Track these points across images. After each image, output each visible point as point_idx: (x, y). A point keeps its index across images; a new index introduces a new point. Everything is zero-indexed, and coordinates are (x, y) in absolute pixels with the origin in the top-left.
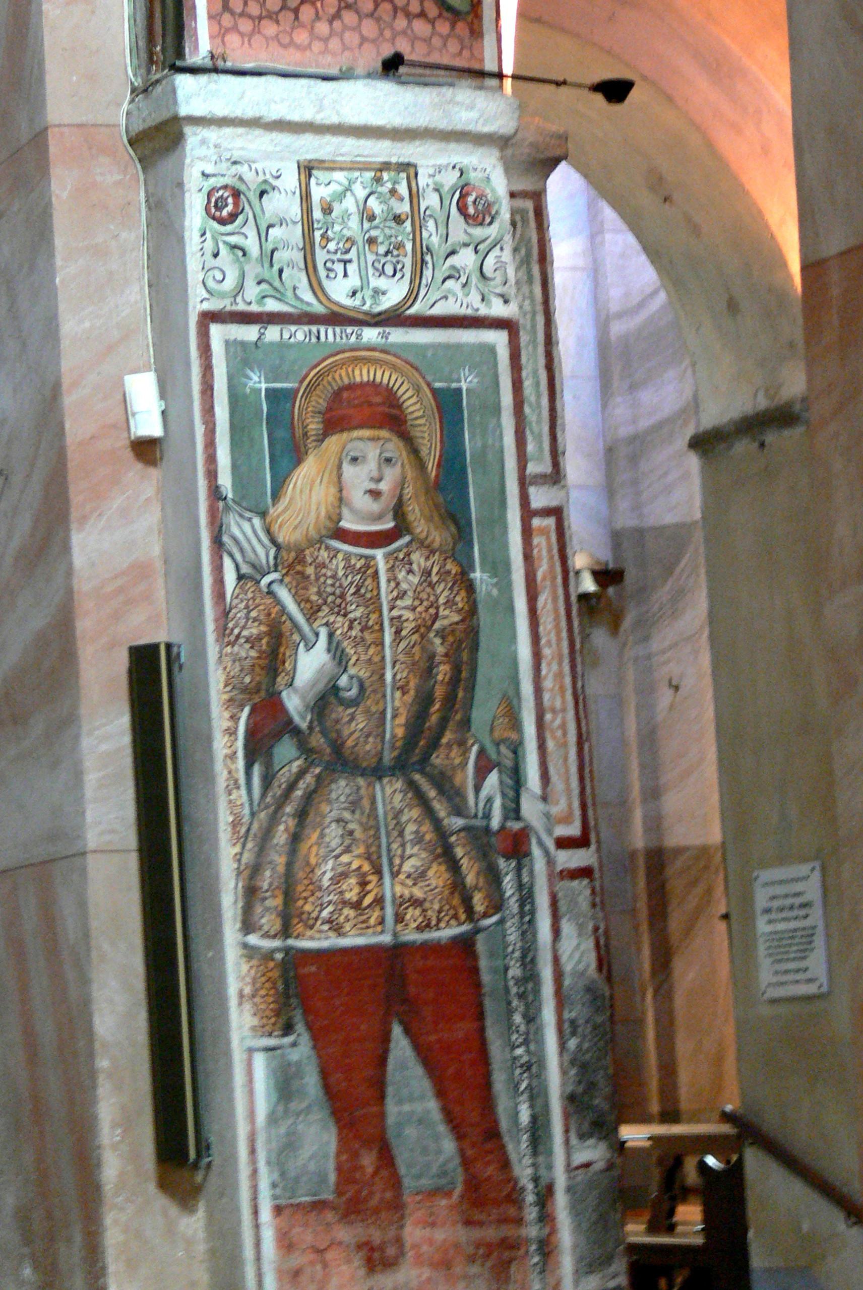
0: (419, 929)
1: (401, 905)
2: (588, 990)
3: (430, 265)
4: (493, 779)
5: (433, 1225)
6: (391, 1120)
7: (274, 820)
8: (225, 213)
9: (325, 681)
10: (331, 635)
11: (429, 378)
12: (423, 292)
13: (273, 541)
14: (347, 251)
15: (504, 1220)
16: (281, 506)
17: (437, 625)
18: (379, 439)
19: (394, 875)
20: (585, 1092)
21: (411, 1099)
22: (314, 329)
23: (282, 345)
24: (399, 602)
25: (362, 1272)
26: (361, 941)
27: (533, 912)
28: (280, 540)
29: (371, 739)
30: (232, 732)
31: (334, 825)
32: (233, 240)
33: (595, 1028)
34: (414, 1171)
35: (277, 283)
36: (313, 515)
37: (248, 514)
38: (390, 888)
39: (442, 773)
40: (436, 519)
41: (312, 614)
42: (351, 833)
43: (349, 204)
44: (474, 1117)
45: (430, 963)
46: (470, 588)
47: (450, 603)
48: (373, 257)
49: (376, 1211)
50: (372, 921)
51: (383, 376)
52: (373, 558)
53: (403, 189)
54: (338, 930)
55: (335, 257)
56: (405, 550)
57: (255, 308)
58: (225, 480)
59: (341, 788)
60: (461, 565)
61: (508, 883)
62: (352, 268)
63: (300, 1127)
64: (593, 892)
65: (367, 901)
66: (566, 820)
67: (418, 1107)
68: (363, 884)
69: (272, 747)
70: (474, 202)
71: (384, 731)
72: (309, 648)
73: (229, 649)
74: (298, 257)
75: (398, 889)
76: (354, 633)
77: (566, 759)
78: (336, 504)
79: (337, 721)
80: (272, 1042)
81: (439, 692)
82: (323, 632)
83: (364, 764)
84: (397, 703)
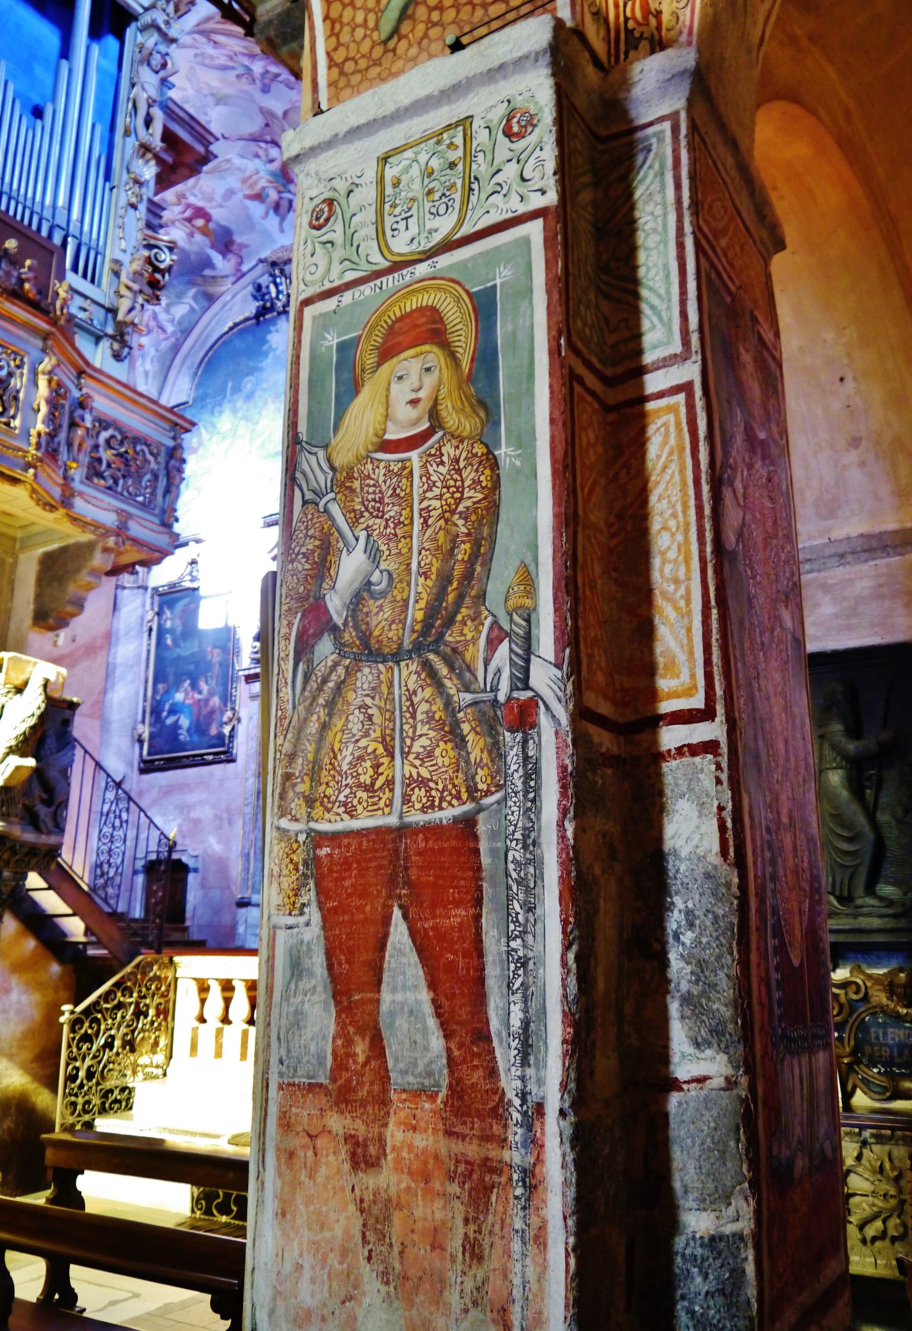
0: (424, 810)
1: (408, 785)
2: (708, 876)
3: (476, 192)
4: (504, 647)
5: (414, 1129)
6: (384, 1008)
7: (309, 711)
8: (322, 221)
9: (360, 579)
10: (369, 536)
11: (467, 287)
12: (469, 213)
13: (333, 468)
14: (410, 209)
15: (486, 1138)
16: (339, 436)
17: (461, 508)
18: (422, 354)
19: (405, 755)
20: (703, 993)
21: (404, 988)
22: (378, 282)
23: (355, 304)
24: (429, 495)
25: (347, 1166)
27: (537, 789)
28: (337, 465)
29: (394, 627)
31: (357, 712)
32: (324, 239)
33: (716, 917)
34: (402, 1066)
35: (355, 258)
36: (363, 436)
37: (315, 450)
38: (400, 769)
39: (454, 650)
40: (468, 409)
41: (354, 523)
42: (370, 718)
43: (415, 171)
44: (464, 1013)
45: (431, 844)
46: (494, 464)
48: (431, 204)
49: (363, 1104)
50: (382, 804)
51: (426, 300)
52: (409, 460)
54: (351, 813)
55: (398, 219)
56: (437, 446)
57: (337, 283)
59: (366, 676)
60: (487, 447)
61: (513, 757)
63: (306, 1006)
64: (719, 767)
65: (378, 784)
66: (689, 692)
67: (410, 996)
68: (376, 766)
69: (313, 646)
70: (518, 122)
71: (406, 618)
73: (290, 566)
75: (408, 769)
76: (388, 530)
77: (689, 630)
78: (382, 419)
79: (367, 614)
80: (291, 921)
81: (458, 570)
82: (363, 535)
83: (387, 651)
84: (420, 589)
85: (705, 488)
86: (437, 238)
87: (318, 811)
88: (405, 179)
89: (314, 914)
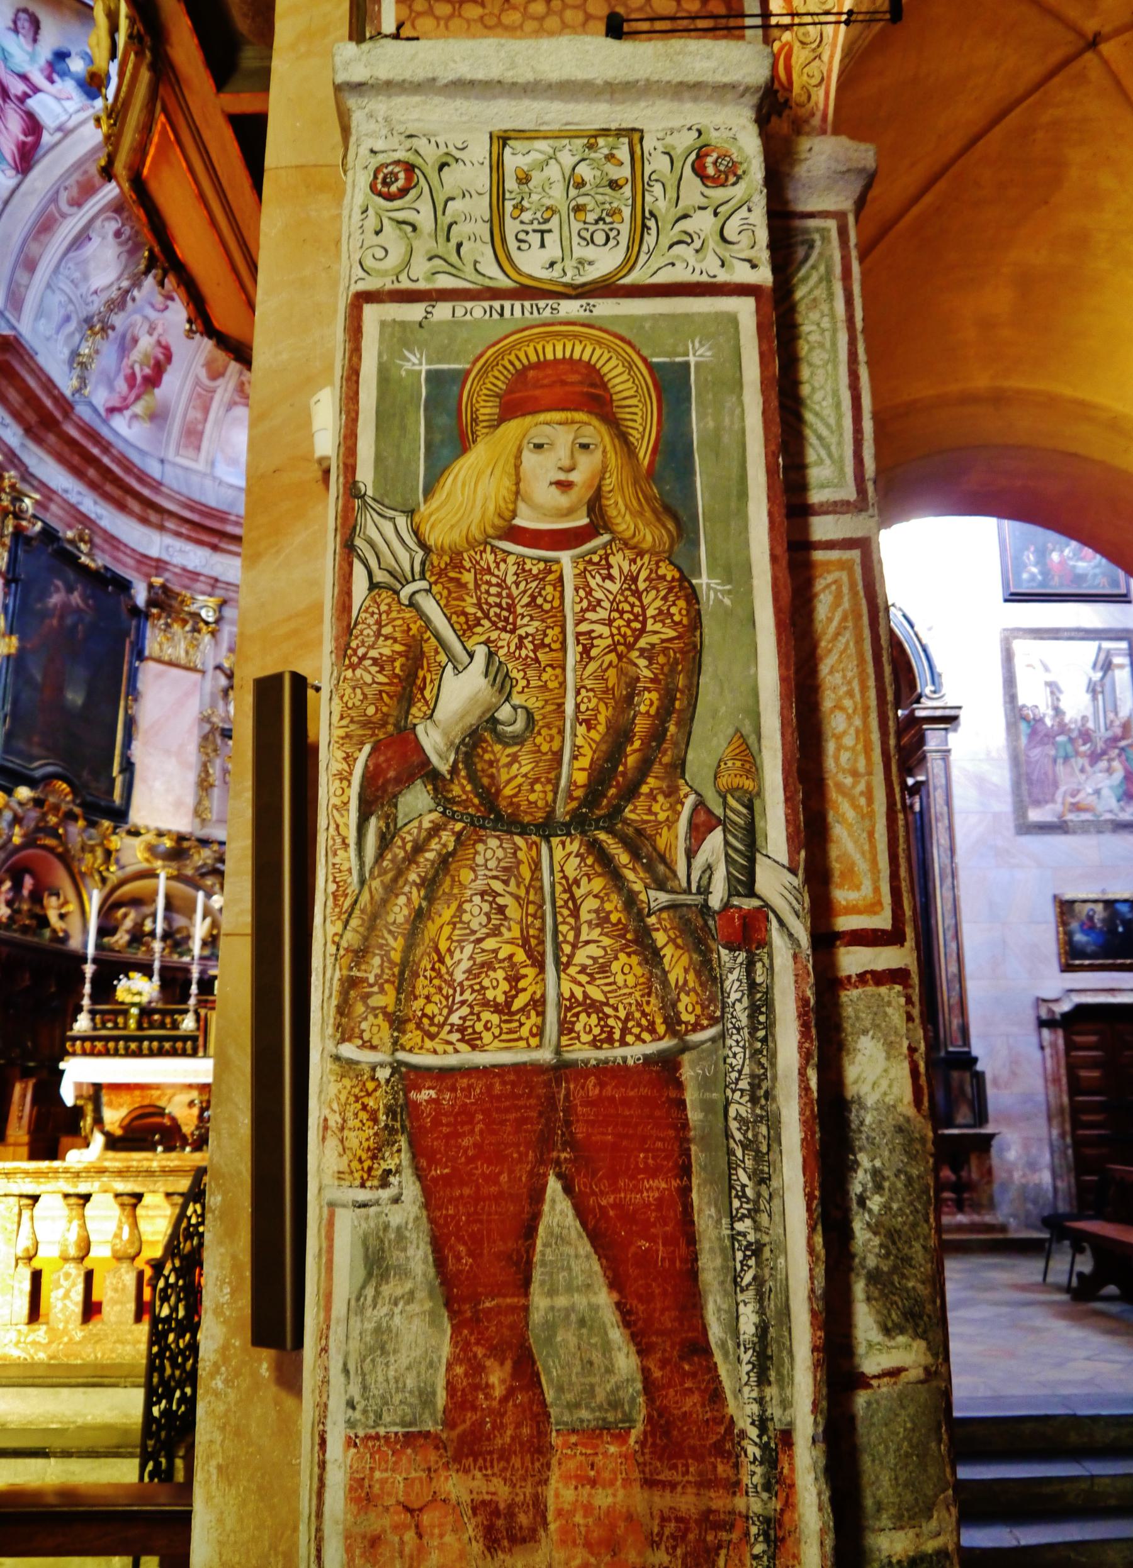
0: (595, 1044)
1: (568, 1009)
2: (900, 1129)
3: (654, 231)
4: (716, 839)
5: (593, 1483)
6: (536, 1318)
7: (391, 890)
8: (394, 189)
9: (478, 712)
10: (491, 655)
11: (644, 353)
12: (643, 258)
13: (422, 545)
14: (547, 221)
15: (706, 1483)
16: (435, 503)
17: (642, 643)
18: (573, 422)
19: (561, 967)
20: (895, 1269)
21: (570, 1289)
22: (497, 304)
23: (455, 324)
24: (588, 615)
25: (477, 1548)
26: (506, 1058)
27: (770, 1026)
28: (431, 542)
29: (538, 787)
30: (345, 778)
31: (477, 899)
32: (400, 216)
33: (910, 1180)
34: (569, 1397)
35: (454, 259)
36: (477, 513)
37: (391, 513)
39: (640, 832)
40: (648, 514)
41: (465, 631)
42: (501, 909)
43: (553, 171)
44: (667, 1320)
45: (608, 1091)
46: (692, 596)
47: (663, 615)
48: (581, 225)
49: (505, 1455)
50: (525, 1032)
51: (582, 352)
52: (557, 561)
53: (623, 154)
54: (473, 1043)
55: (529, 228)
56: (601, 552)
57: (422, 285)
58: (365, 475)
60: (680, 570)
61: (734, 983)
62: (551, 239)
63: (397, 1320)
64: (909, 1001)
65: (518, 1004)
66: (873, 908)
67: (581, 1301)
68: (514, 979)
69: (395, 796)
70: (715, 163)
71: (558, 778)
72: (457, 671)
73: (349, 674)
74: (484, 230)
75: (566, 987)
76: (524, 653)
77: (871, 834)
78: (512, 497)
79: (491, 763)
80: (363, 1195)
81: (641, 726)
82: (481, 652)
83: (527, 819)
84: (579, 741)
85: (887, 670)
86: (592, 274)
87: (412, 1036)
88: (537, 178)
89: (410, 1188)
